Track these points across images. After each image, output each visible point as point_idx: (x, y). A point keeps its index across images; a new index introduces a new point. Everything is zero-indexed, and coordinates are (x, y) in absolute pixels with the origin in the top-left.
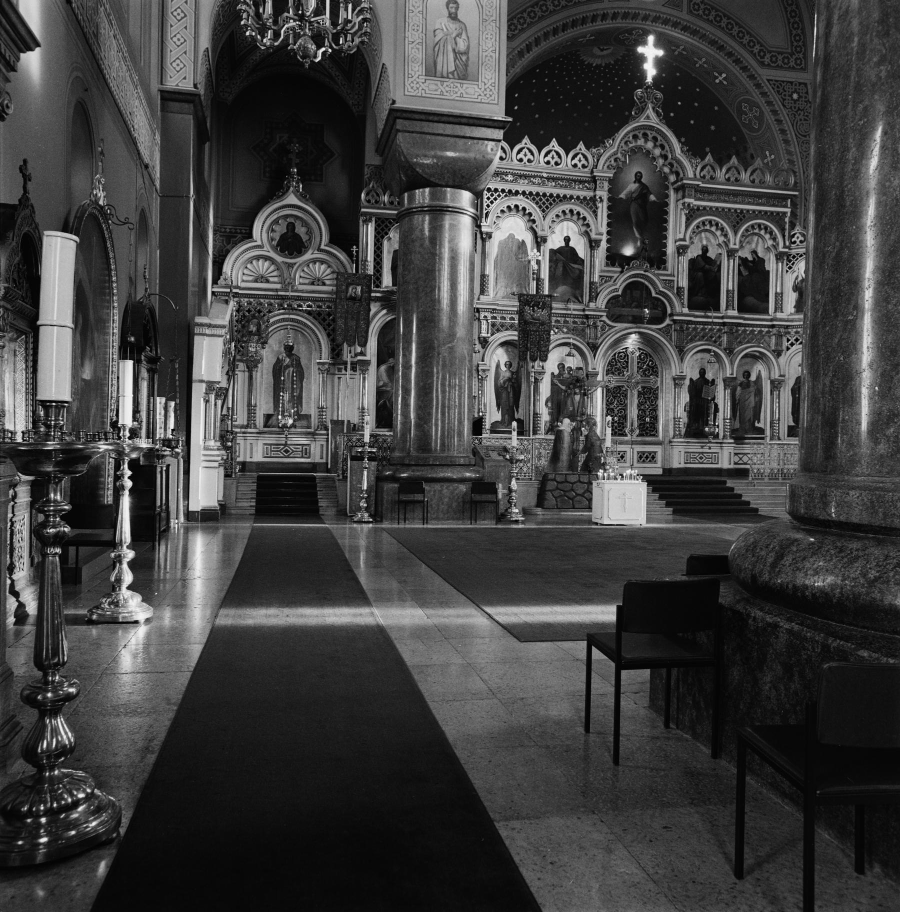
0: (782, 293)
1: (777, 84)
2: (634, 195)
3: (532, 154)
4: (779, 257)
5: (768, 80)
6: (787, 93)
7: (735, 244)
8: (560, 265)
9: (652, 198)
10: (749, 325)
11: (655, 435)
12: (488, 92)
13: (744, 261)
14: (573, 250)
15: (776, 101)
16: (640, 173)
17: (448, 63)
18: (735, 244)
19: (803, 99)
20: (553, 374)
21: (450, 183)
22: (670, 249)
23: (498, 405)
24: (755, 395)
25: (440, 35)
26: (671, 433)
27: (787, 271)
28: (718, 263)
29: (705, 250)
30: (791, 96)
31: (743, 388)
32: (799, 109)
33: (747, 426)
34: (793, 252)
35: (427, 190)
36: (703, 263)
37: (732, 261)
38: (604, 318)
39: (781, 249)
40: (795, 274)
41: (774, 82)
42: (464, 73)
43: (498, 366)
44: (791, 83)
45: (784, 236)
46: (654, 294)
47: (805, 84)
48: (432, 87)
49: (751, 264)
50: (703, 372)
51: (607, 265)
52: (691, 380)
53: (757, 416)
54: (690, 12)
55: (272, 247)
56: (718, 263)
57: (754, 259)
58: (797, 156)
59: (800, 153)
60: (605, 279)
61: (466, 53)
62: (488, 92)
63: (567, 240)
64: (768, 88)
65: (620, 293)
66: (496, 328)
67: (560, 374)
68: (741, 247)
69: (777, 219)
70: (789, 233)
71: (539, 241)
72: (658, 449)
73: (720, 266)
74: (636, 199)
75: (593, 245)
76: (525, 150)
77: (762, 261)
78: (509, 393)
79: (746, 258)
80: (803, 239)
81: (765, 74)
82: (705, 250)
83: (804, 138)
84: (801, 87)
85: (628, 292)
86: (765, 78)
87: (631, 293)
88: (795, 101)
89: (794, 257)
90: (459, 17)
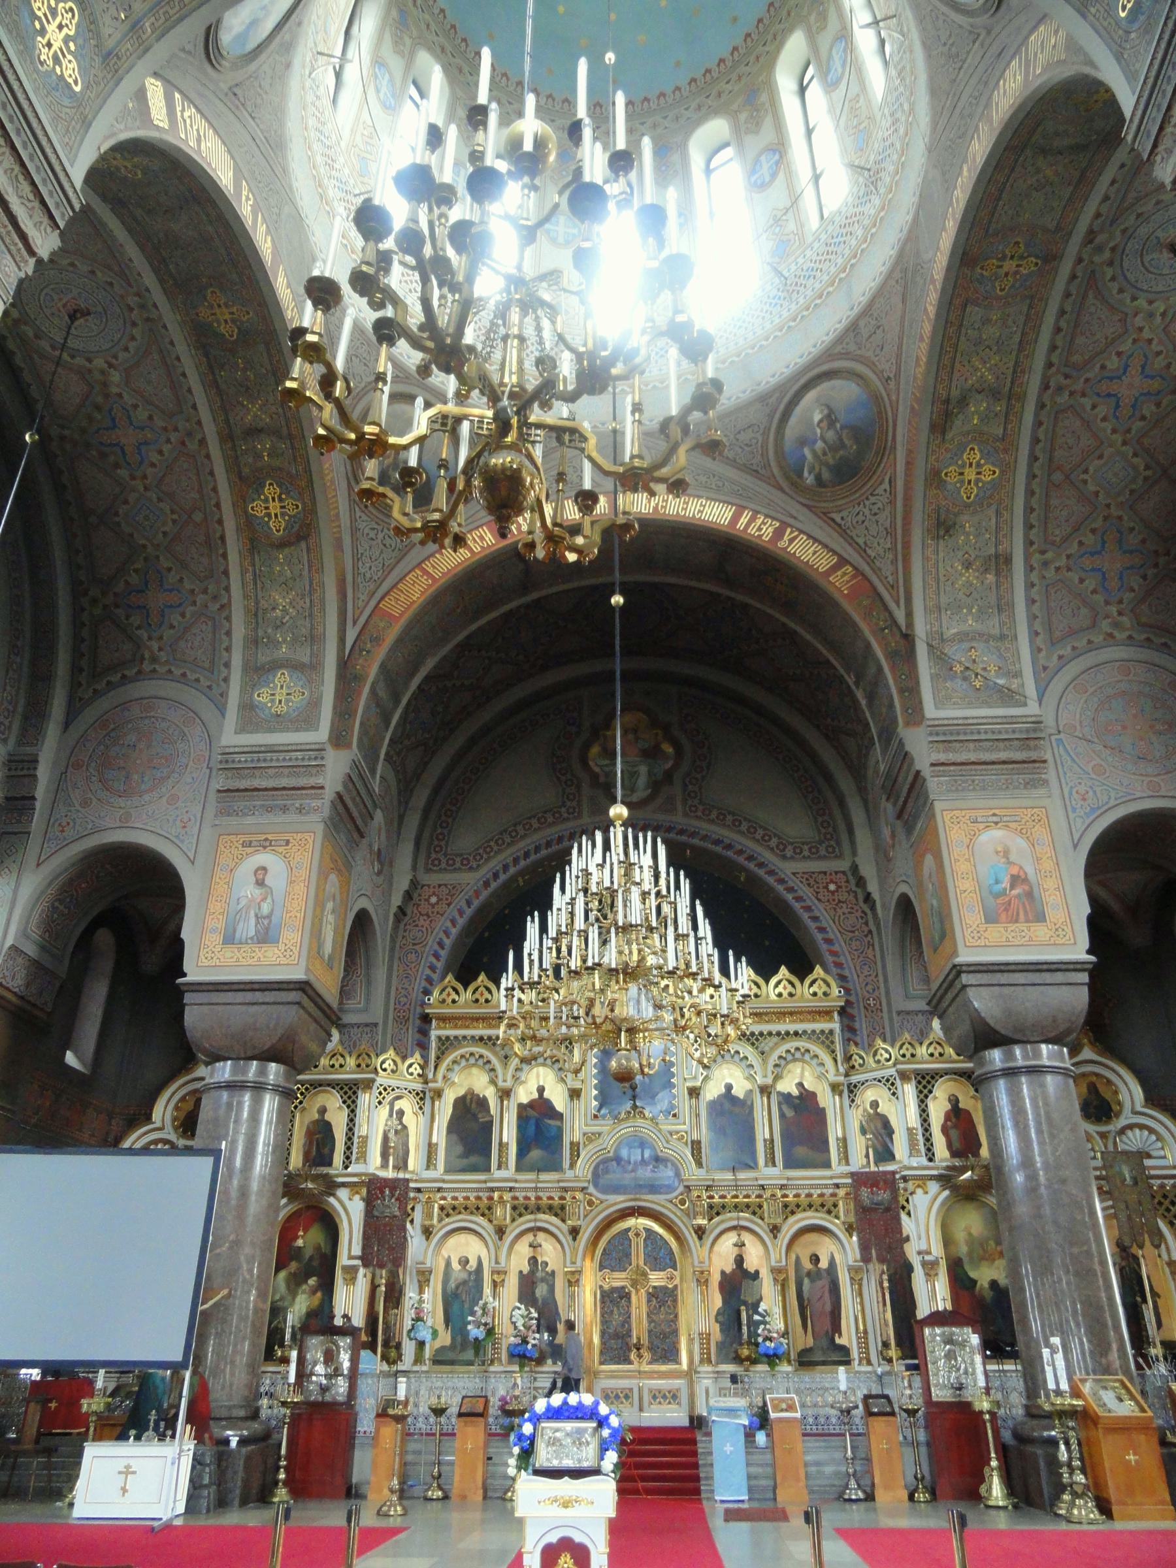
0: (844, 1140)
3: (490, 992)
4: (835, 1088)
5: (794, 874)
7: (765, 1076)
8: (533, 1122)
10: (803, 1187)
11: (677, 1361)
12: (288, 953)
13: (786, 1098)
17: (248, 928)
20: (521, 1272)
21: (243, 1056)
22: (680, 1091)
24: (830, 1291)
25: (243, 902)
26: (697, 1358)
29: (729, 1087)
30: (826, 887)
31: (812, 1281)
32: (840, 901)
33: (824, 1342)
34: (854, 1079)
35: (229, 1062)
36: (727, 1105)
37: (765, 1099)
38: (592, 1189)
39: (832, 1077)
42: (266, 936)
43: (448, 1263)
44: (825, 873)
45: (835, 1060)
47: (844, 873)
48: (229, 955)
49: (797, 1101)
50: (739, 1260)
52: (723, 1273)
53: (836, 1328)
54: (686, 815)
55: (176, 1129)
56: (749, 1103)
57: (801, 1094)
60: (590, 1138)
61: (269, 917)
62: (288, 953)
63: (541, 1090)
64: (792, 882)
67: (532, 1272)
68: (777, 1078)
69: (825, 1039)
70: (845, 1054)
71: (505, 1094)
72: (679, 1383)
75: (575, 1094)
76: (482, 989)
77: (813, 1095)
79: (789, 1094)
81: (788, 868)
82: (729, 1087)
83: (851, 935)
86: (789, 873)
88: (833, 893)
89: (855, 1086)
90: (269, 881)
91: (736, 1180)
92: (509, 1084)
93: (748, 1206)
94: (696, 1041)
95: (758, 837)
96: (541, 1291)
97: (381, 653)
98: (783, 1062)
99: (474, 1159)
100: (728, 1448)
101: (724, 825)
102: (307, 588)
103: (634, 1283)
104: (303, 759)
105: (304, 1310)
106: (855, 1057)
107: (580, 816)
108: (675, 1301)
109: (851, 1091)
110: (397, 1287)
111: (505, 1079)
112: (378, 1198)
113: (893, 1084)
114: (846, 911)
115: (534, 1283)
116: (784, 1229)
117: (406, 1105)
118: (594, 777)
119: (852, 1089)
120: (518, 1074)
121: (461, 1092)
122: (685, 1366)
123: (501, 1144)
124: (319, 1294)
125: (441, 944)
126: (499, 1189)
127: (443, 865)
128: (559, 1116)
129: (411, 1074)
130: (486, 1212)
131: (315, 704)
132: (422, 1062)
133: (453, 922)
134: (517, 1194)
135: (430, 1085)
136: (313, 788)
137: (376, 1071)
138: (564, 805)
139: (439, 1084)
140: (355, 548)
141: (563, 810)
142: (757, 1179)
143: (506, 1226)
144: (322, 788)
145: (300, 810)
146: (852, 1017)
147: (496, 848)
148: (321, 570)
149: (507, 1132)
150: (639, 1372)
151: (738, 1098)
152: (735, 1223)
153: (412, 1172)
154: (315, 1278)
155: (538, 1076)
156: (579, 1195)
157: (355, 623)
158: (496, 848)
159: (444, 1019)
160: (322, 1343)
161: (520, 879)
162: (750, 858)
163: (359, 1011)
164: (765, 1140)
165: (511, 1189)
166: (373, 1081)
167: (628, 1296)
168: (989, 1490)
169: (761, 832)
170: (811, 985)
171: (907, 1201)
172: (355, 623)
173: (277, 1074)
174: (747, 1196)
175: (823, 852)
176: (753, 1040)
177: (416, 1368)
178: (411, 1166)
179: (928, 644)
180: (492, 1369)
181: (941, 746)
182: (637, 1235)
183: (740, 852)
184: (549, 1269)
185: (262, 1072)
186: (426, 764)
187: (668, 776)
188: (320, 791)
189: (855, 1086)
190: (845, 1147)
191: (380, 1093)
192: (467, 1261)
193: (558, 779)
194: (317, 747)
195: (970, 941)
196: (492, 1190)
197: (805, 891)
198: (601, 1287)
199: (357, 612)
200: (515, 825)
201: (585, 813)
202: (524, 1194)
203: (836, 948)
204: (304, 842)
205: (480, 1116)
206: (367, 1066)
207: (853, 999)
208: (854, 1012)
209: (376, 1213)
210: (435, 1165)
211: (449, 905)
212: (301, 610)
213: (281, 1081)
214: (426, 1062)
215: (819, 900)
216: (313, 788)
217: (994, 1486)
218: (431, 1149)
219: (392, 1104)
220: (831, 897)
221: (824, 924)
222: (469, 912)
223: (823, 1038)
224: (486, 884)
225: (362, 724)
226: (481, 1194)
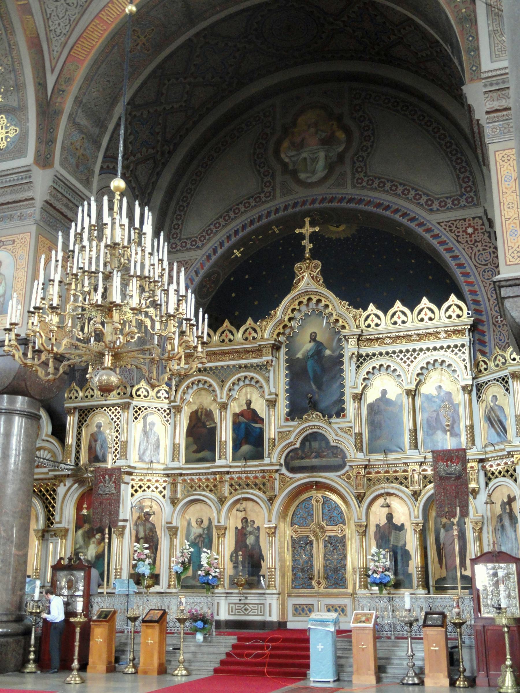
0: (472, 427)
1: (448, 224)
2: (310, 353)
5: (439, 223)
6: (461, 230)
8: (243, 426)
9: (328, 352)
11: (345, 586)
13: (429, 398)
14: (254, 412)
15: (449, 239)
16: (314, 333)
19: (480, 231)
20: (237, 528)
22: (348, 398)
26: (357, 585)
27: (478, 401)
29: (384, 393)
30: (465, 231)
34: (481, 380)
37: (411, 400)
38: (284, 470)
40: (484, 405)
41: (445, 223)
43: (189, 524)
44: (464, 220)
45: (466, 367)
47: (480, 218)
50: (390, 517)
51: (287, 420)
52: (377, 526)
54: (354, 187)
58: (479, 285)
59: (483, 281)
60: (283, 435)
65: (298, 445)
71: (224, 407)
72: (346, 601)
73: (401, 406)
74: (312, 356)
75: (272, 404)
80: (485, 366)
81: (433, 219)
82: (384, 393)
83: (486, 267)
84: (475, 221)
85: (307, 444)
87: (310, 444)
88: (470, 235)
91: (387, 460)
92: (225, 400)
93: (397, 479)
94: (358, 360)
95: (410, 196)
96: (250, 540)
97: (74, 90)
98: (425, 372)
100: (320, 647)
101: (384, 191)
102: (8, 49)
103: (316, 535)
104: (18, 179)
105: (94, 555)
106: (482, 363)
107: (274, 198)
108: (344, 546)
109: (478, 390)
110: (155, 540)
111: (222, 396)
112: (102, 482)
113: (507, 382)
114: (481, 249)
115: (246, 535)
116: (423, 493)
117: (156, 419)
118: (285, 165)
119: (479, 388)
120: (232, 393)
121: (195, 408)
122: (350, 590)
123: (221, 441)
126: (219, 473)
127: (179, 248)
128: (262, 420)
129: (159, 398)
130: (213, 488)
131: (23, 137)
132: (167, 389)
134: (233, 476)
135: (172, 404)
136: (26, 200)
138: (263, 192)
139: (178, 403)
140: (44, 12)
141: (262, 195)
142: (401, 459)
143: (226, 498)
144: (32, 199)
145: (21, 217)
146: (483, 333)
147: (214, 230)
148: (13, 32)
150: (318, 594)
152: (382, 491)
154: (99, 534)
155: (246, 394)
156: (277, 476)
157: (53, 71)
158: (214, 230)
160: (66, 576)
161: (235, 251)
162: (404, 215)
164: (410, 430)
165: (228, 473)
166: (129, 404)
167: (311, 543)
168: (504, 681)
169: (413, 193)
170: (447, 310)
171: (515, 470)
172: (53, 71)
173: (22, 403)
174: (396, 471)
175: (463, 203)
176: (401, 356)
177: (168, 591)
179: (486, 4)
180: (216, 591)
181: (495, 95)
182: (317, 501)
183: (396, 211)
184: (255, 526)
185: (12, 402)
186: (159, 174)
187: (341, 157)
188: (31, 202)
189: (481, 386)
190: (473, 433)
192: (202, 522)
193: (259, 171)
194: (25, 169)
195: (510, 260)
196: (215, 473)
197: (448, 237)
198: (292, 536)
199: (53, 64)
200: (228, 212)
201: (278, 196)
202: (237, 475)
203: (472, 279)
204: (24, 240)
205: (208, 423)
206: (124, 394)
207: (484, 318)
208: (485, 328)
209: (101, 493)
210: (179, 460)
212: (7, 66)
213: (26, 408)
214: (170, 389)
215: (459, 242)
216: (26, 200)
217: (507, 678)
218: (175, 448)
220: (469, 239)
221: (463, 261)
223: (456, 350)
224: (209, 258)
225: (63, 148)
226: (209, 477)
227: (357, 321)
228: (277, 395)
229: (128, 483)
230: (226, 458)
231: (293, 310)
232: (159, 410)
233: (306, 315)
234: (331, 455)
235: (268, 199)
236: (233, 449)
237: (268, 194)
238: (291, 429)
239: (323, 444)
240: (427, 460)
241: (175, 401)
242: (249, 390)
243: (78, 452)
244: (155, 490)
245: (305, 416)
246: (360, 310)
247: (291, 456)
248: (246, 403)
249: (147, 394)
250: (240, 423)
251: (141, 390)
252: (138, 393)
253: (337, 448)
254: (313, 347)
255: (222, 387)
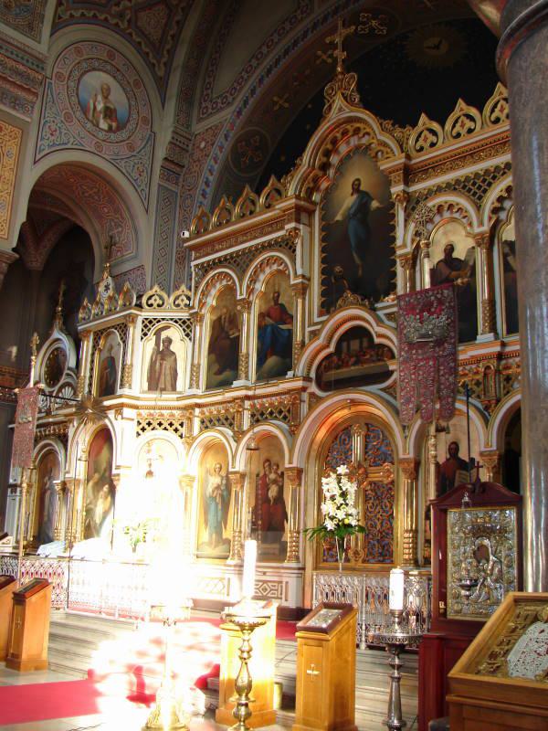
2: (352, 211)
8: (269, 329)
9: (375, 204)
14: (282, 306)
16: (358, 180)
18: (481, 224)
23: (206, 522)
28: (471, 263)
29: (450, 249)
38: (313, 388)
46: (377, 340)
51: (320, 315)
56: (471, 263)
65: (332, 349)
66: (205, 425)
71: (247, 304)
74: (354, 215)
78: (217, 504)
82: (450, 249)
85: (345, 344)
99: (227, 374)
124: (109, 498)
125: (207, 184)
129: (178, 305)
133: (215, 160)
135: (191, 312)
137: (139, 306)
149: (249, 344)
151: (460, 260)
153: (180, 393)
158: (245, 77)
159: (196, 248)
163: (132, 258)
178: (178, 390)
191: (146, 326)
205: (231, 333)
211: (212, 145)
218: (195, 368)
219: (158, 334)
222: (227, 145)
224: (239, 113)
227: (404, 146)
228: (309, 280)
229: (133, 420)
230: (247, 378)
231: (327, 154)
232: (176, 322)
233: (348, 156)
234: (374, 358)
235: (304, 15)
236: (257, 364)
237: (305, 9)
238: (318, 327)
239: (365, 344)
240: (508, 349)
241: (193, 308)
242: (277, 281)
243: (90, 385)
244: (168, 427)
245: (339, 302)
246: (408, 127)
247: (325, 368)
248: (274, 298)
249: (161, 303)
250: (266, 326)
251: (153, 298)
252: (150, 302)
253: (382, 346)
254: (355, 201)
255: (241, 280)
